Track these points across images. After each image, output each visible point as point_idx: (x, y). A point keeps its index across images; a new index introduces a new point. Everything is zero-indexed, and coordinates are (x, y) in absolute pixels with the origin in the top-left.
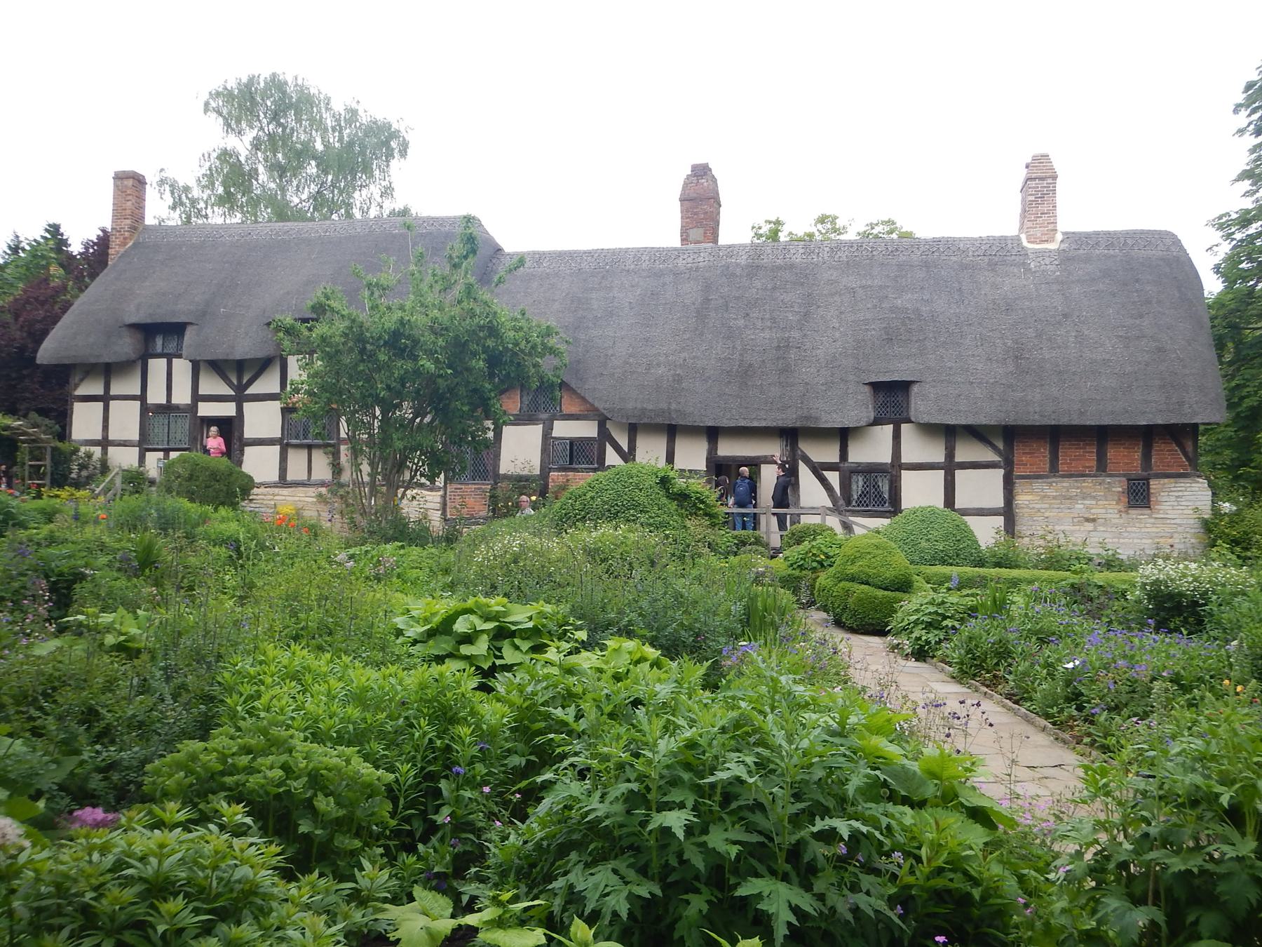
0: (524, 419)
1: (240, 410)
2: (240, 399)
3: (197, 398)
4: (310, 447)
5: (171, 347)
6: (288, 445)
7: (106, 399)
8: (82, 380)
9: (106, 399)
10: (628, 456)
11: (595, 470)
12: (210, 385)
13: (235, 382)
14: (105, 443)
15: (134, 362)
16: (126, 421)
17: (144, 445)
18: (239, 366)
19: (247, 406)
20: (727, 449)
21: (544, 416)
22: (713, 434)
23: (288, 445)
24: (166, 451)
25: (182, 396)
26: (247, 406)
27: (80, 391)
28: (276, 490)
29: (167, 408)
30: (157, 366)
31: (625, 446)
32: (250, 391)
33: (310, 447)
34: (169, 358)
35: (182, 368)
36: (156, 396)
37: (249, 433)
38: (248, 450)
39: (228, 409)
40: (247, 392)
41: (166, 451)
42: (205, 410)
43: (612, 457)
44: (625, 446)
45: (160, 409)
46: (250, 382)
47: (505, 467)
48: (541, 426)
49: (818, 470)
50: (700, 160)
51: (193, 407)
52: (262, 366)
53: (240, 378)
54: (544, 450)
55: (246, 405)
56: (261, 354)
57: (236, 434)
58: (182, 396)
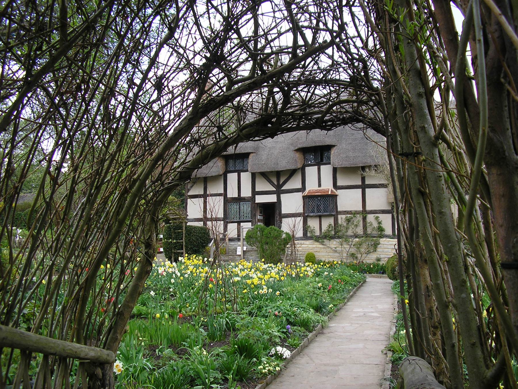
1: (279, 198)
2: (279, 192)
3: (255, 193)
4: (320, 217)
5: (239, 167)
6: (308, 216)
7: (205, 196)
8: (192, 187)
9: (205, 196)
12: (262, 185)
13: (276, 183)
14: (205, 219)
15: (221, 175)
16: (217, 207)
17: (226, 220)
18: (278, 174)
19: (283, 197)
23: (308, 216)
24: (239, 223)
25: (246, 192)
26: (283, 197)
27: (190, 193)
28: (303, 242)
29: (239, 199)
30: (232, 177)
33: (320, 217)
34: (239, 172)
35: (246, 177)
36: (232, 193)
37: (284, 211)
38: (284, 220)
39: (272, 199)
41: (239, 223)
42: (260, 199)
45: (234, 200)
46: (285, 183)
51: (253, 198)
52: (292, 173)
53: (278, 181)
56: (293, 167)
57: (277, 212)
58: (246, 192)
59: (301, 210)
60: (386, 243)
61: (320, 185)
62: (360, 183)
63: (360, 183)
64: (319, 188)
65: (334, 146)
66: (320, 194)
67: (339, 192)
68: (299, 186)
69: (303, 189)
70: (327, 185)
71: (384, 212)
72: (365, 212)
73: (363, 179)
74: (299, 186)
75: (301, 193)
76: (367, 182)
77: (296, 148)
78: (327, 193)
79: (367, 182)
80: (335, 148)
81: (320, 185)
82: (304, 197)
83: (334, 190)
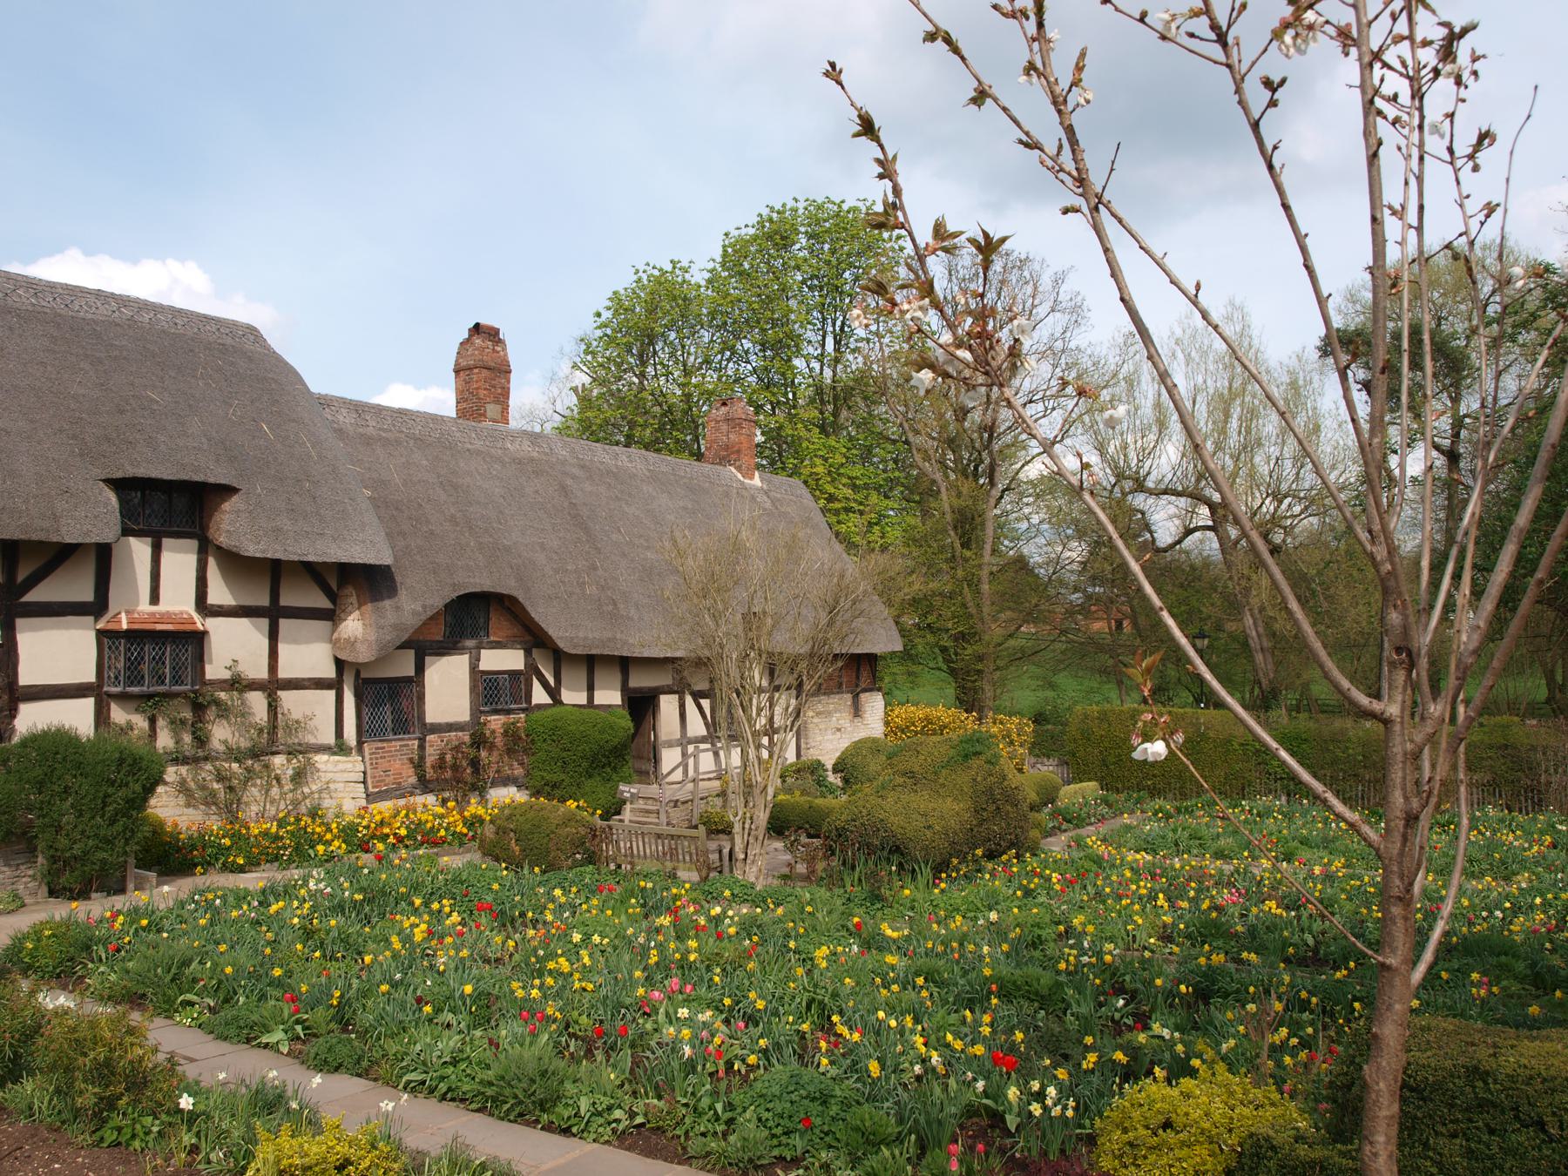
0: (446, 648)
10: (554, 693)
11: (523, 710)
20: (639, 681)
21: (470, 643)
22: (625, 664)
31: (552, 681)
32: (32, 596)
40: (23, 599)
43: (539, 696)
44: (552, 681)
47: (432, 716)
48: (466, 657)
49: (697, 696)
50: (484, 321)
54: (473, 689)
55: (20, 622)
59: (91, 677)
60: (330, 767)
61: (155, 598)
62: (265, 601)
63: (265, 601)
64: (154, 608)
65: (228, 491)
66: (170, 627)
67: (213, 625)
68: (86, 594)
69: (98, 607)
70: (178, 601)
71: (319, 684)
72: (273, 686)
73: (275, 596)
74: (86, 594)
75: (91, 619)
76: (285, 601)
77: (119, 475)
78: (188, 627)
79: (285, 601)
80: (235, 498)
81: (155, 598)
82: (101, 634)
83: (196, 617)
